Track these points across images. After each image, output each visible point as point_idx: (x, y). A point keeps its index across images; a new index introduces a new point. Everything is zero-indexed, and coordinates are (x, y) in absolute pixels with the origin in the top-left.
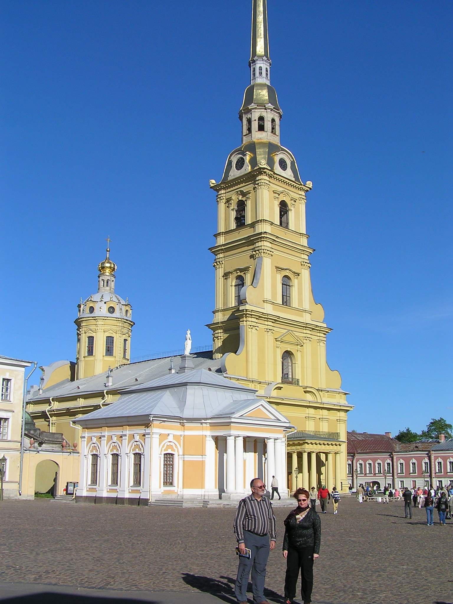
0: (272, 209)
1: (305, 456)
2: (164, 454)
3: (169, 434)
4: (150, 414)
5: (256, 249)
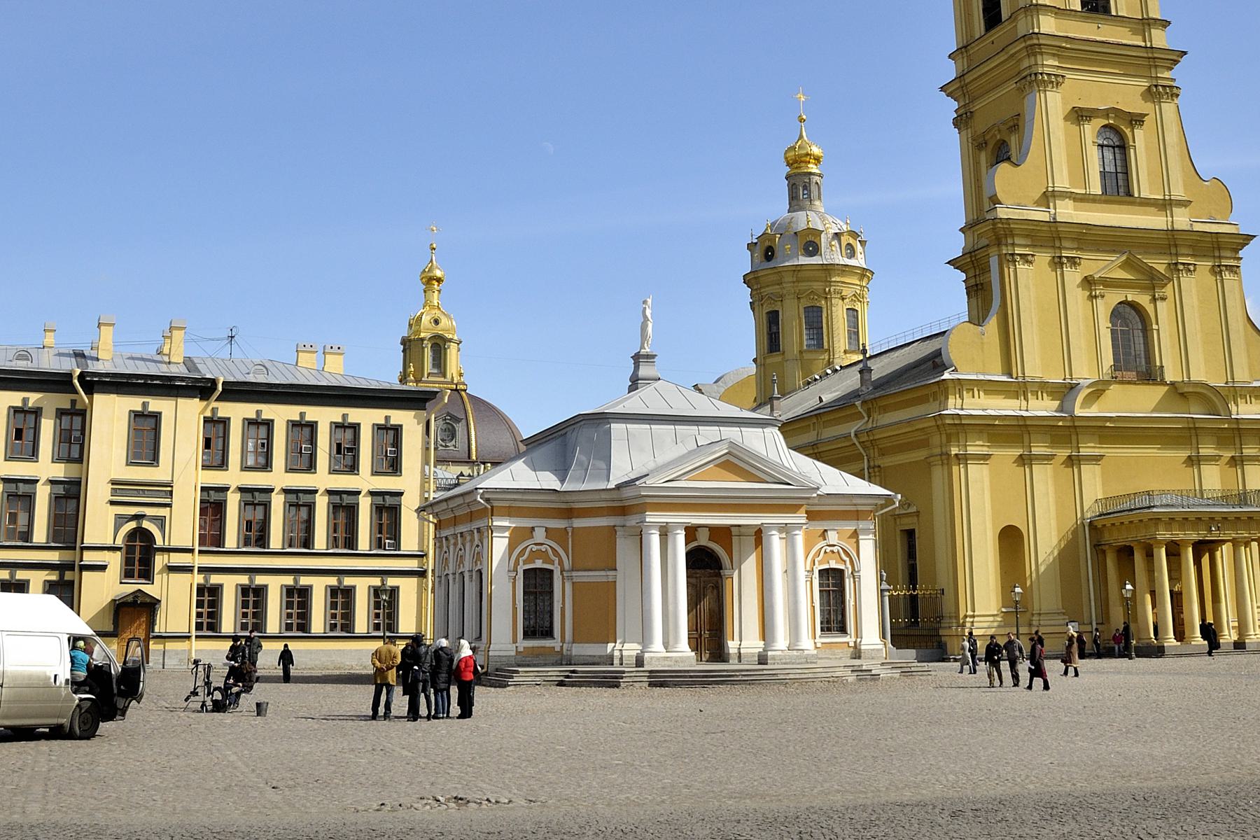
2: (525, 571)
3: (533, 528)
4: (476, 489)
5: (1024, 75)
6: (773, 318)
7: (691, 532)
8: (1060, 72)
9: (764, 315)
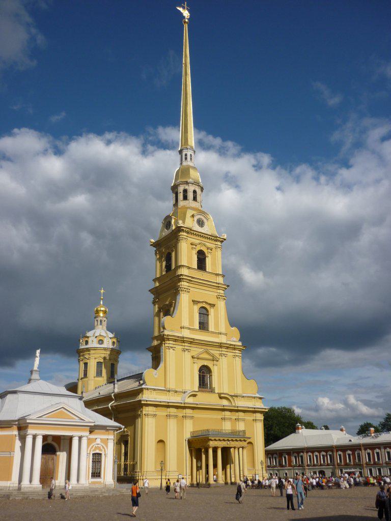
0: (190, 258)
1: (211, 452)
7: (45, 438)
8: (188, 288)
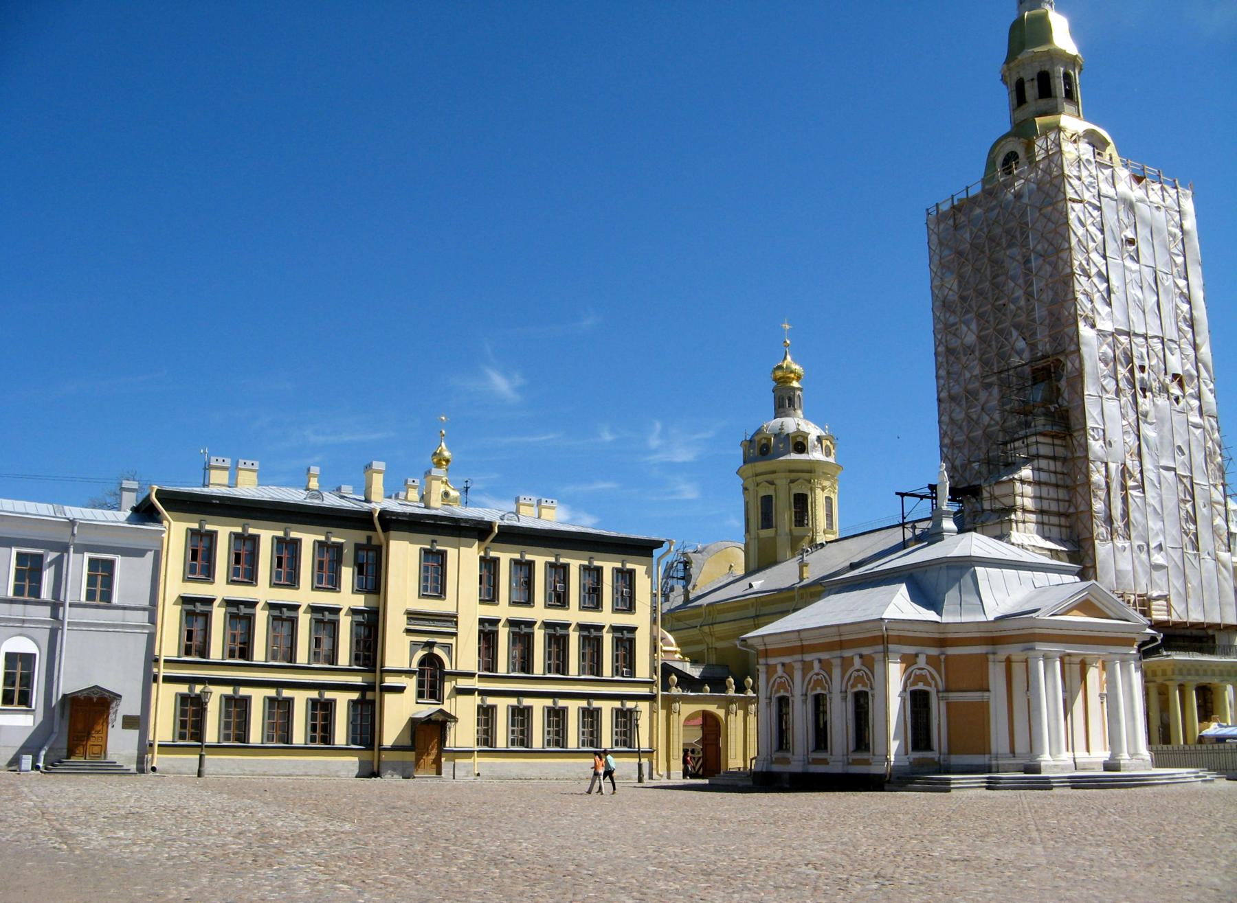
3: (916, 655)
4: (882, 619)
6: (767, 502)
9: (759, 500)
